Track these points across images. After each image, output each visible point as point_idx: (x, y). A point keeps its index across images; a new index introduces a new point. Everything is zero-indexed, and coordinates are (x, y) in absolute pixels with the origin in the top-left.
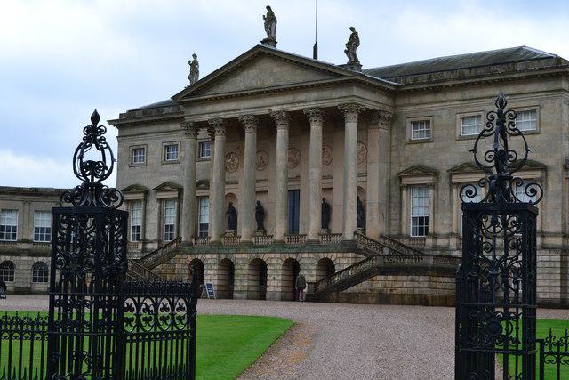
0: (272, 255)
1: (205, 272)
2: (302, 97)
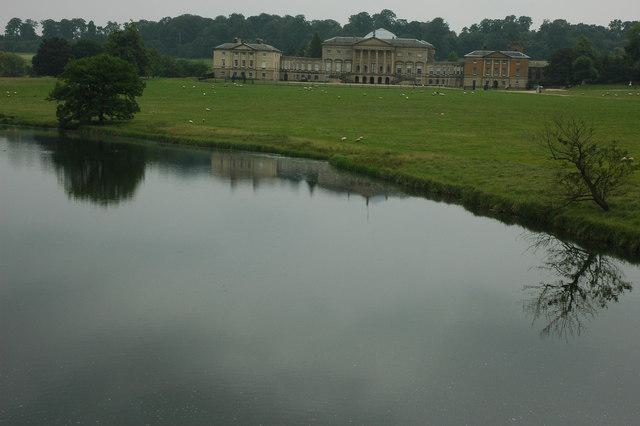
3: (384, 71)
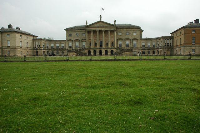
2: (107, 28)
3: (110, 46)
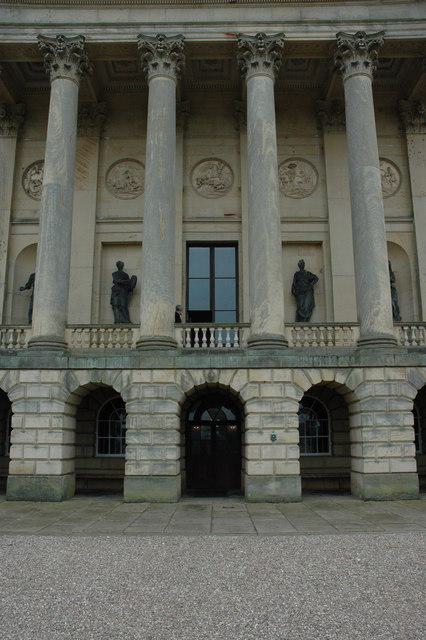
0: (264, 375)
1: (15, 421)
